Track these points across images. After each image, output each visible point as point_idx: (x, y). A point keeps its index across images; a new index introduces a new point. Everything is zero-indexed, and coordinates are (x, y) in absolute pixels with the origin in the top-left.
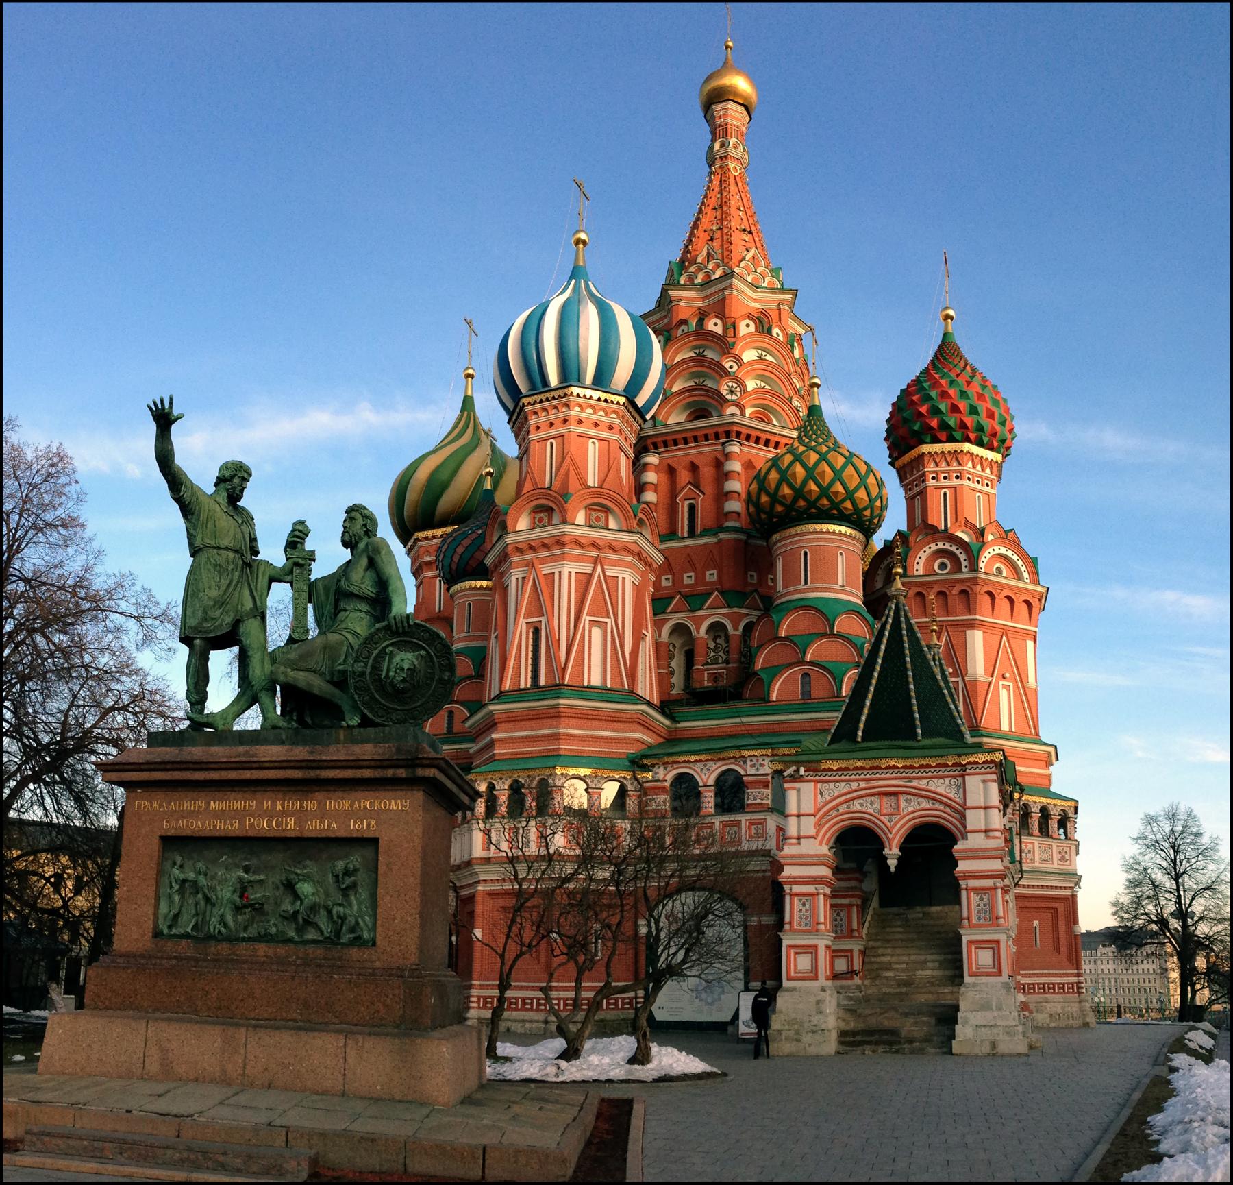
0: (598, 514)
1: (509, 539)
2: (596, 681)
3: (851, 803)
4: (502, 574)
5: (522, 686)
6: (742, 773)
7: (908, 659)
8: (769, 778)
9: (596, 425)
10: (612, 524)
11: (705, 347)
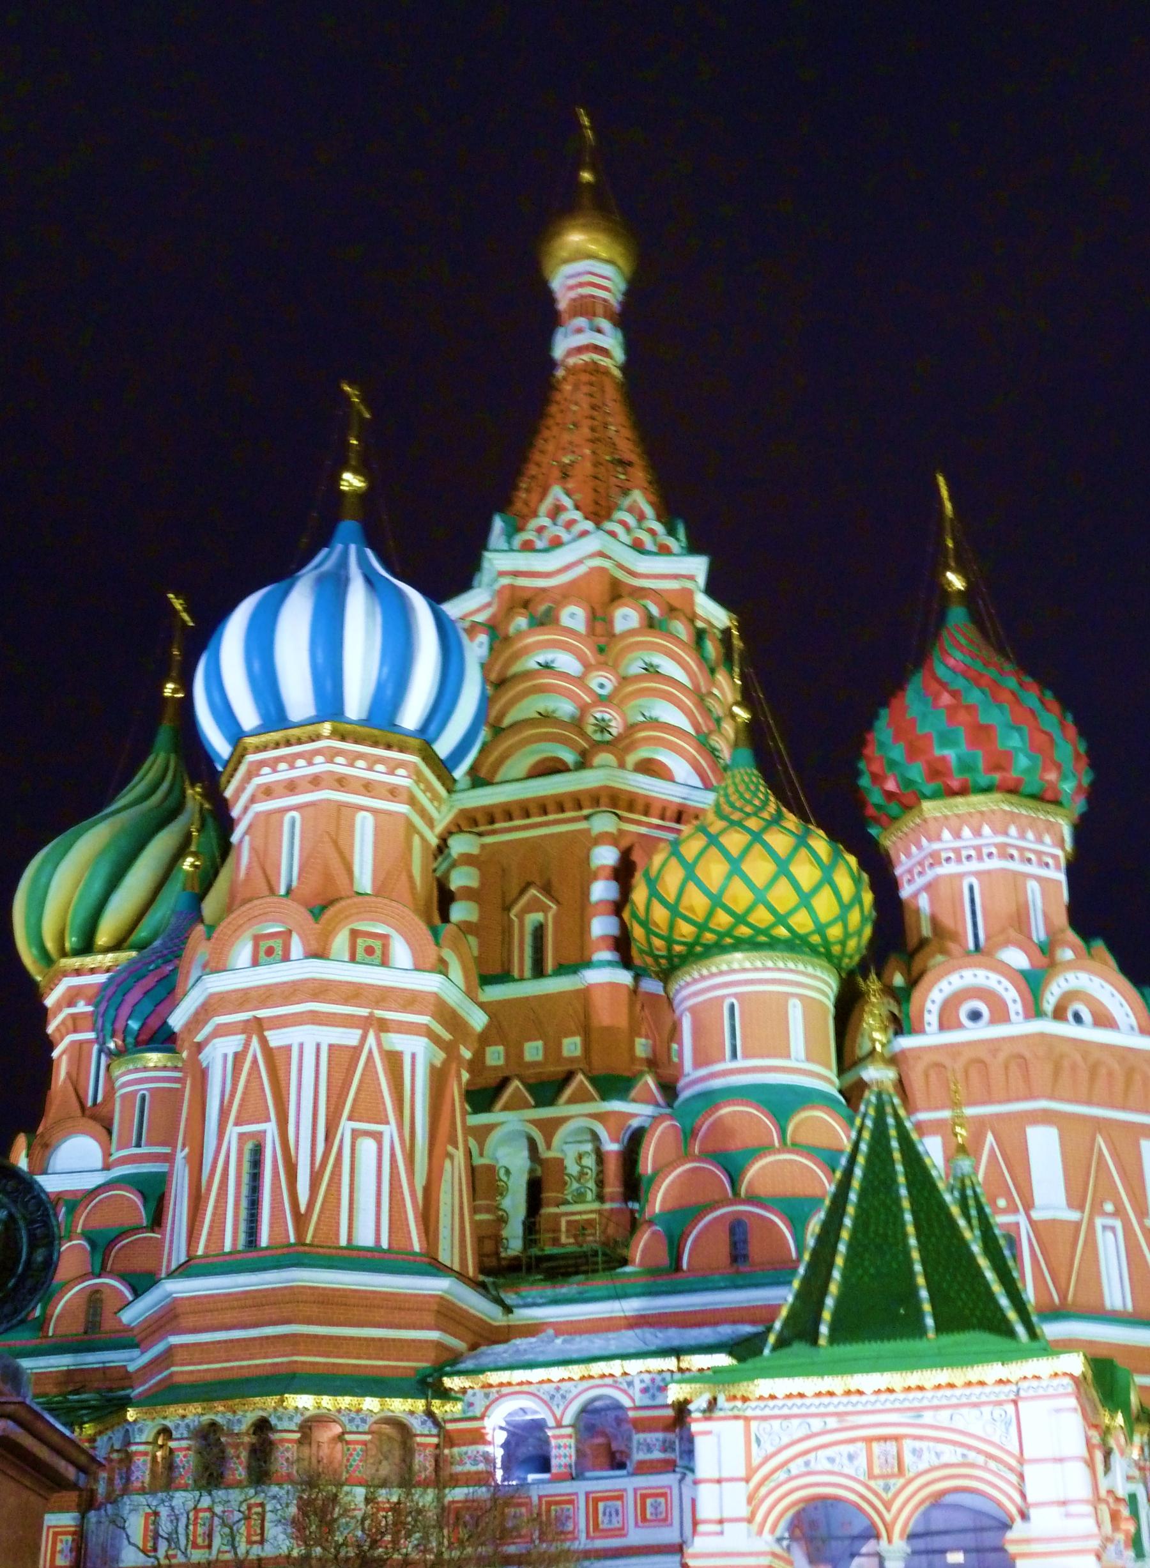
0: (370, 942)
2: (365, 1237)
3: (811, 1456)
4: (200, 1047)
5: (228, 1248)
6: (627, 1402)
9: (368, 788)
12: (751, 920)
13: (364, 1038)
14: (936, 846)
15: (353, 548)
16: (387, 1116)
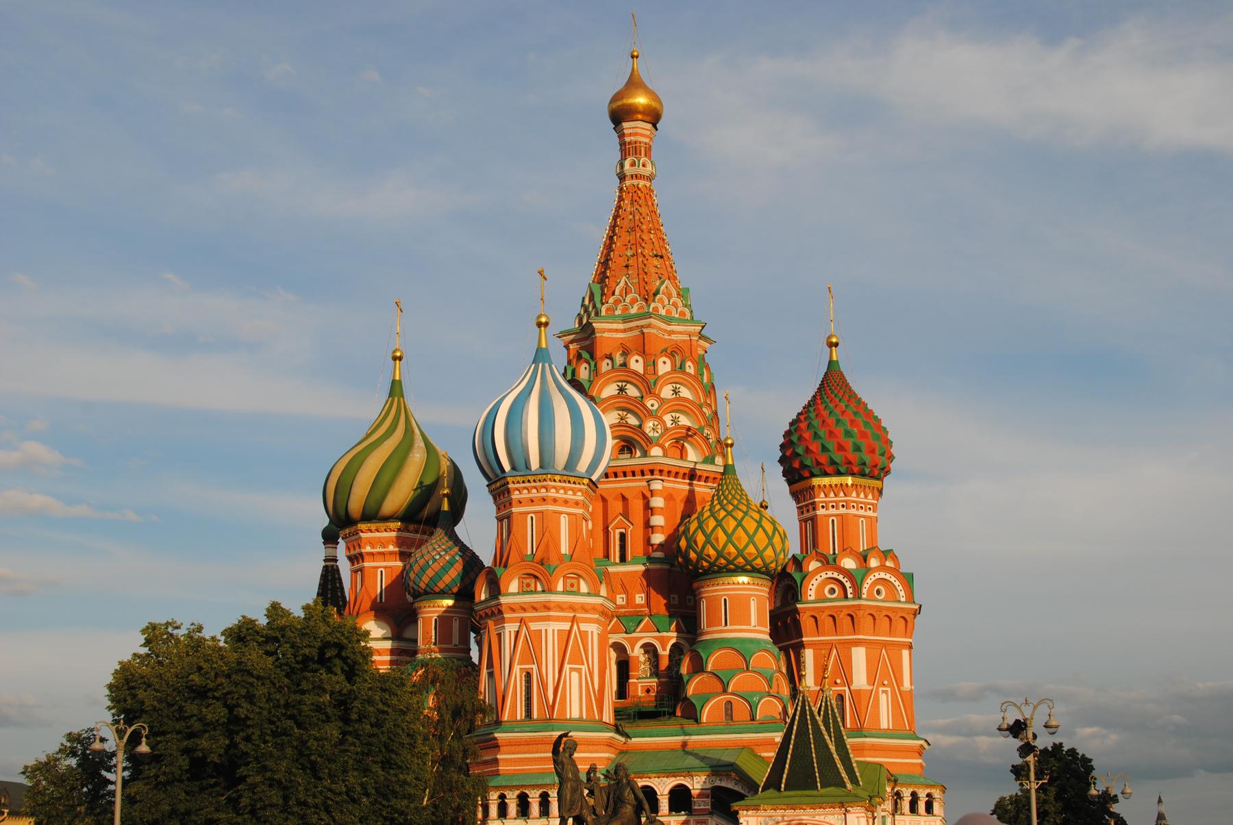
1: (503, 600)
2: (576, 714)
5: (519, 718)
6: (691, 788)
7: (811, 736)
8: (709, 791)
10: (584, 588)
11: (628, 382)
12: (735, 562)
13: (572, 627)
14: (816, 500)
15: (547, 365)
16: (583, 662)
